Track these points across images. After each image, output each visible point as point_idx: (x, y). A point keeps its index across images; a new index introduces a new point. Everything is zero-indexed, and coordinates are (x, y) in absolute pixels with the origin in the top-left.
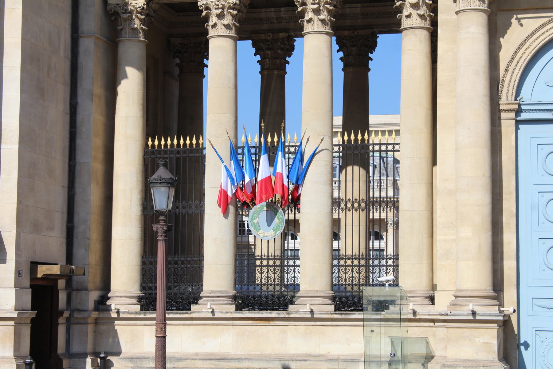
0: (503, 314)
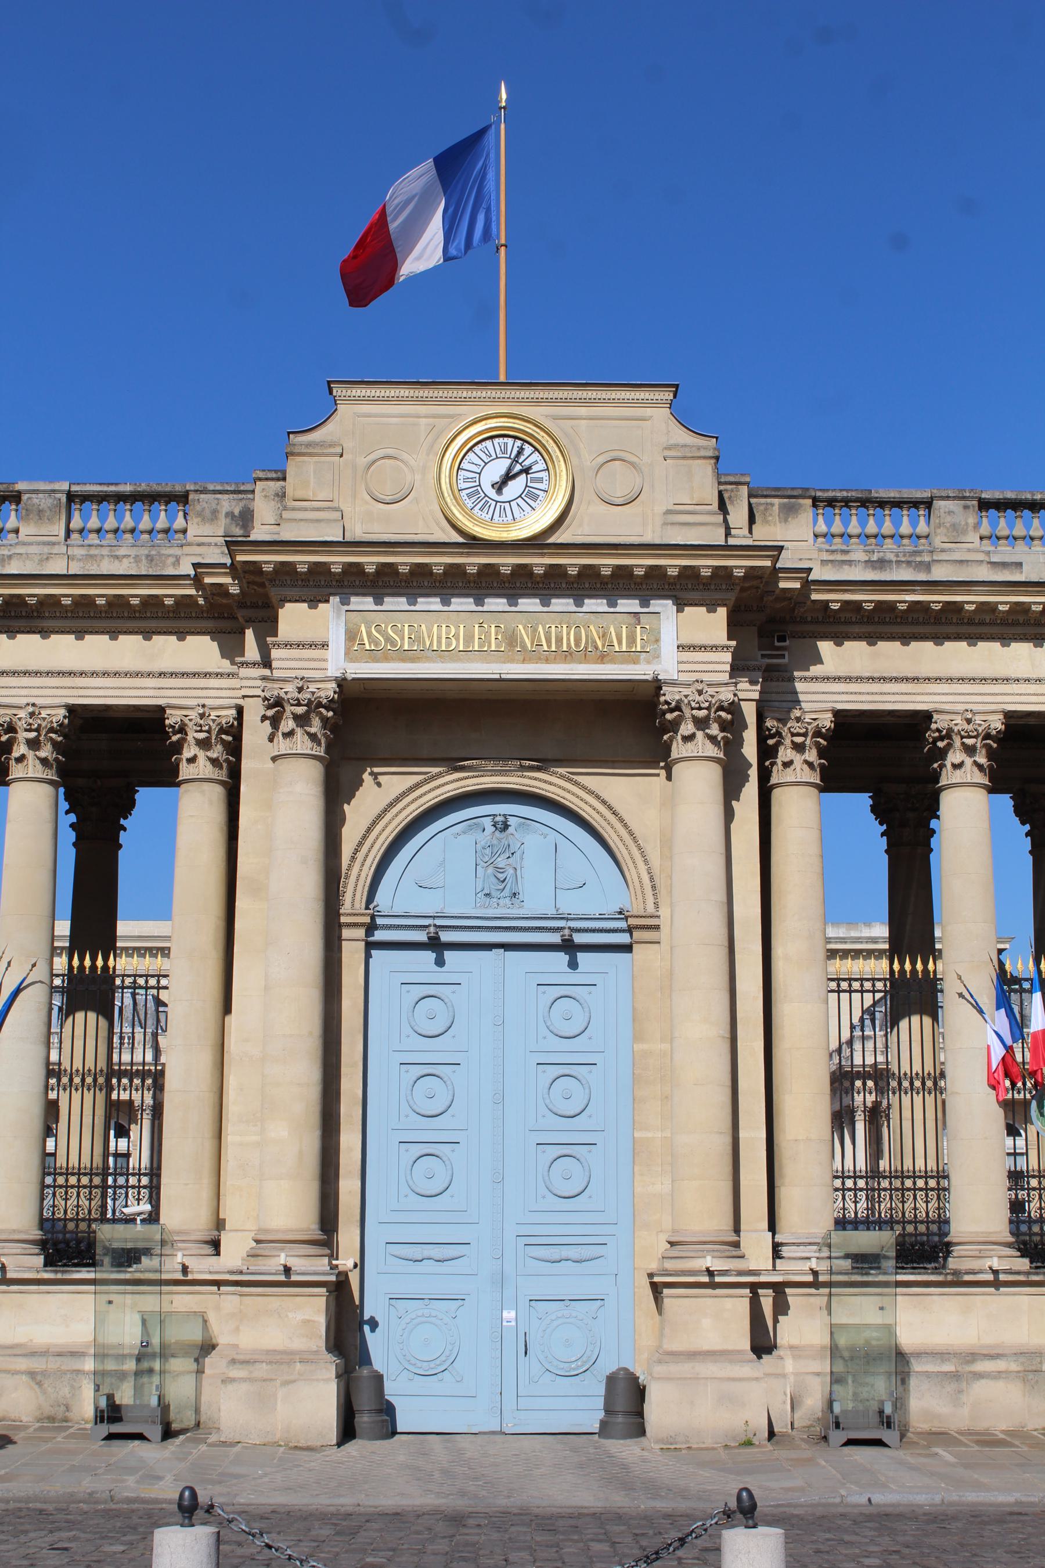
0: (336, 1271)
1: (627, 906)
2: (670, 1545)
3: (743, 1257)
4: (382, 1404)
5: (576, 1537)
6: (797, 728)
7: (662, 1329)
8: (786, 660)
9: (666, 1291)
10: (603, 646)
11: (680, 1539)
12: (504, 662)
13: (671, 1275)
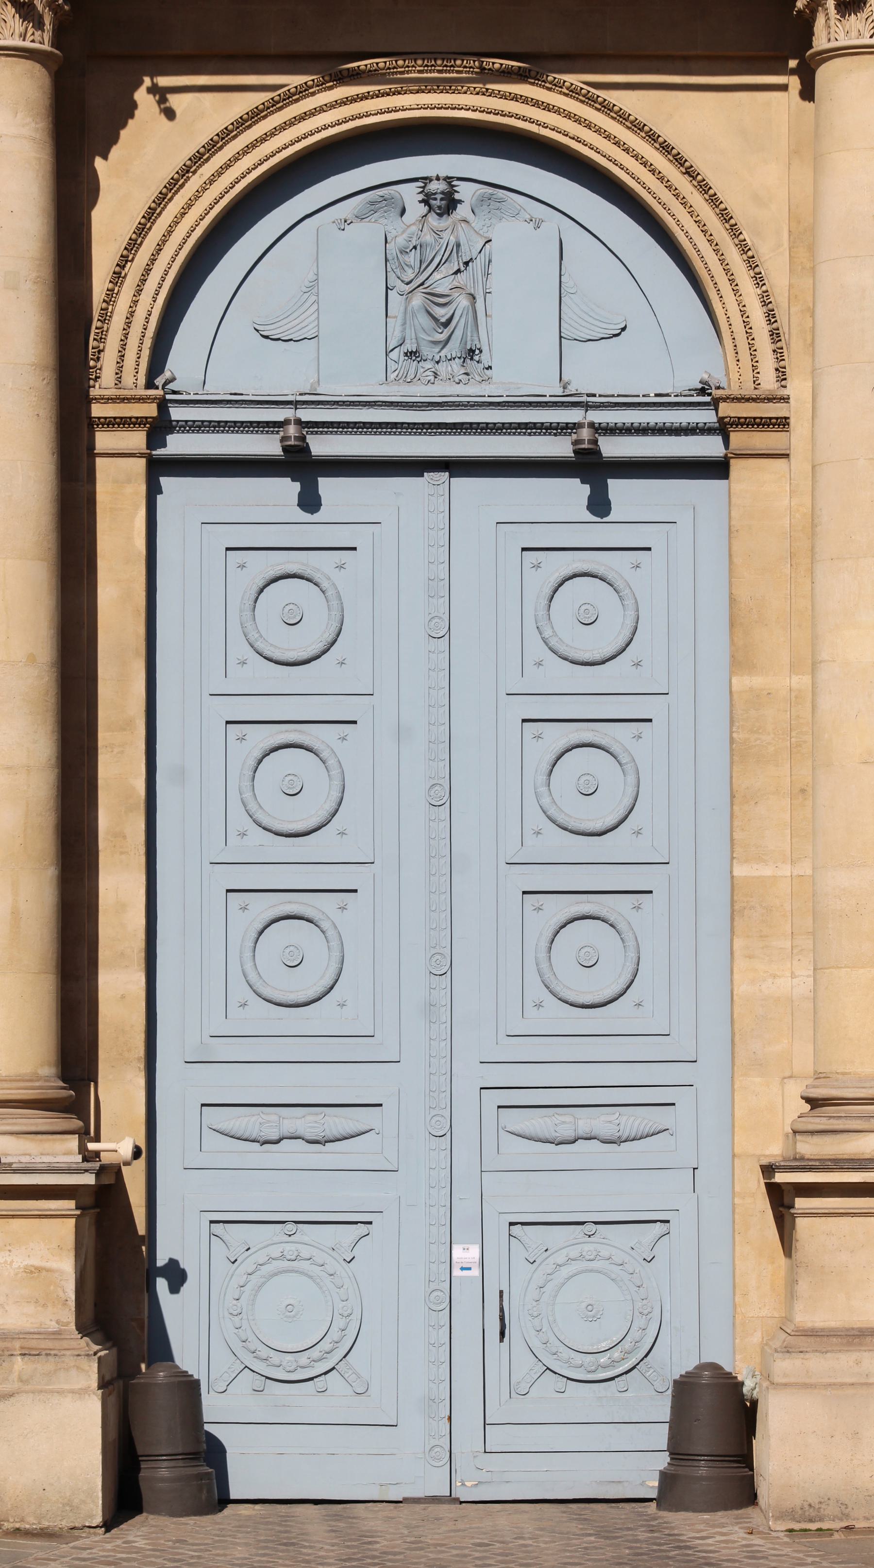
0: (97, 1165)
1: (717, 376)
4: (198, 1441)
7: (792, 1282)
9: (801, 1203)
13: (811, 1169)
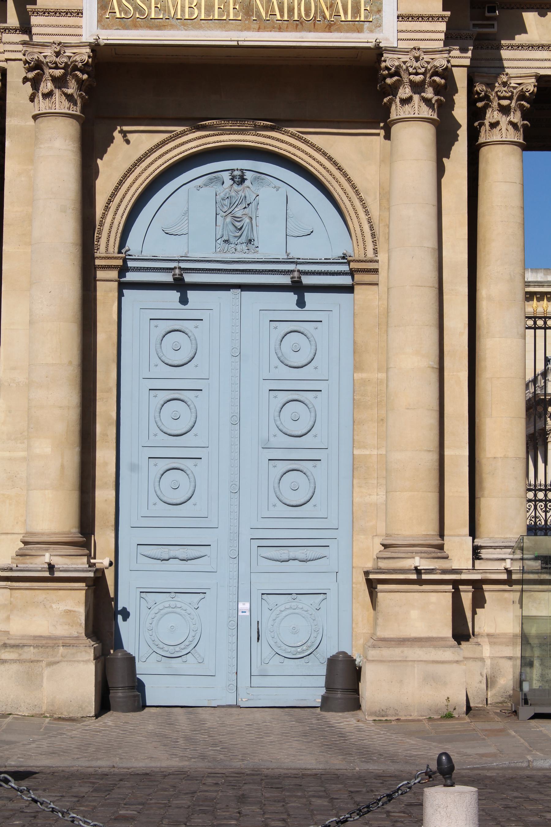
0: (94, 569)
1: (350, 252)
2: (379, 800)
3: (447, 558)
5: (299, 794)
6: (504, 92)
7: (376, 619)
8: (495, 30)
9: (380, 587)
10: (331, 16)
11: (388, 795)
12: (241, 30)
